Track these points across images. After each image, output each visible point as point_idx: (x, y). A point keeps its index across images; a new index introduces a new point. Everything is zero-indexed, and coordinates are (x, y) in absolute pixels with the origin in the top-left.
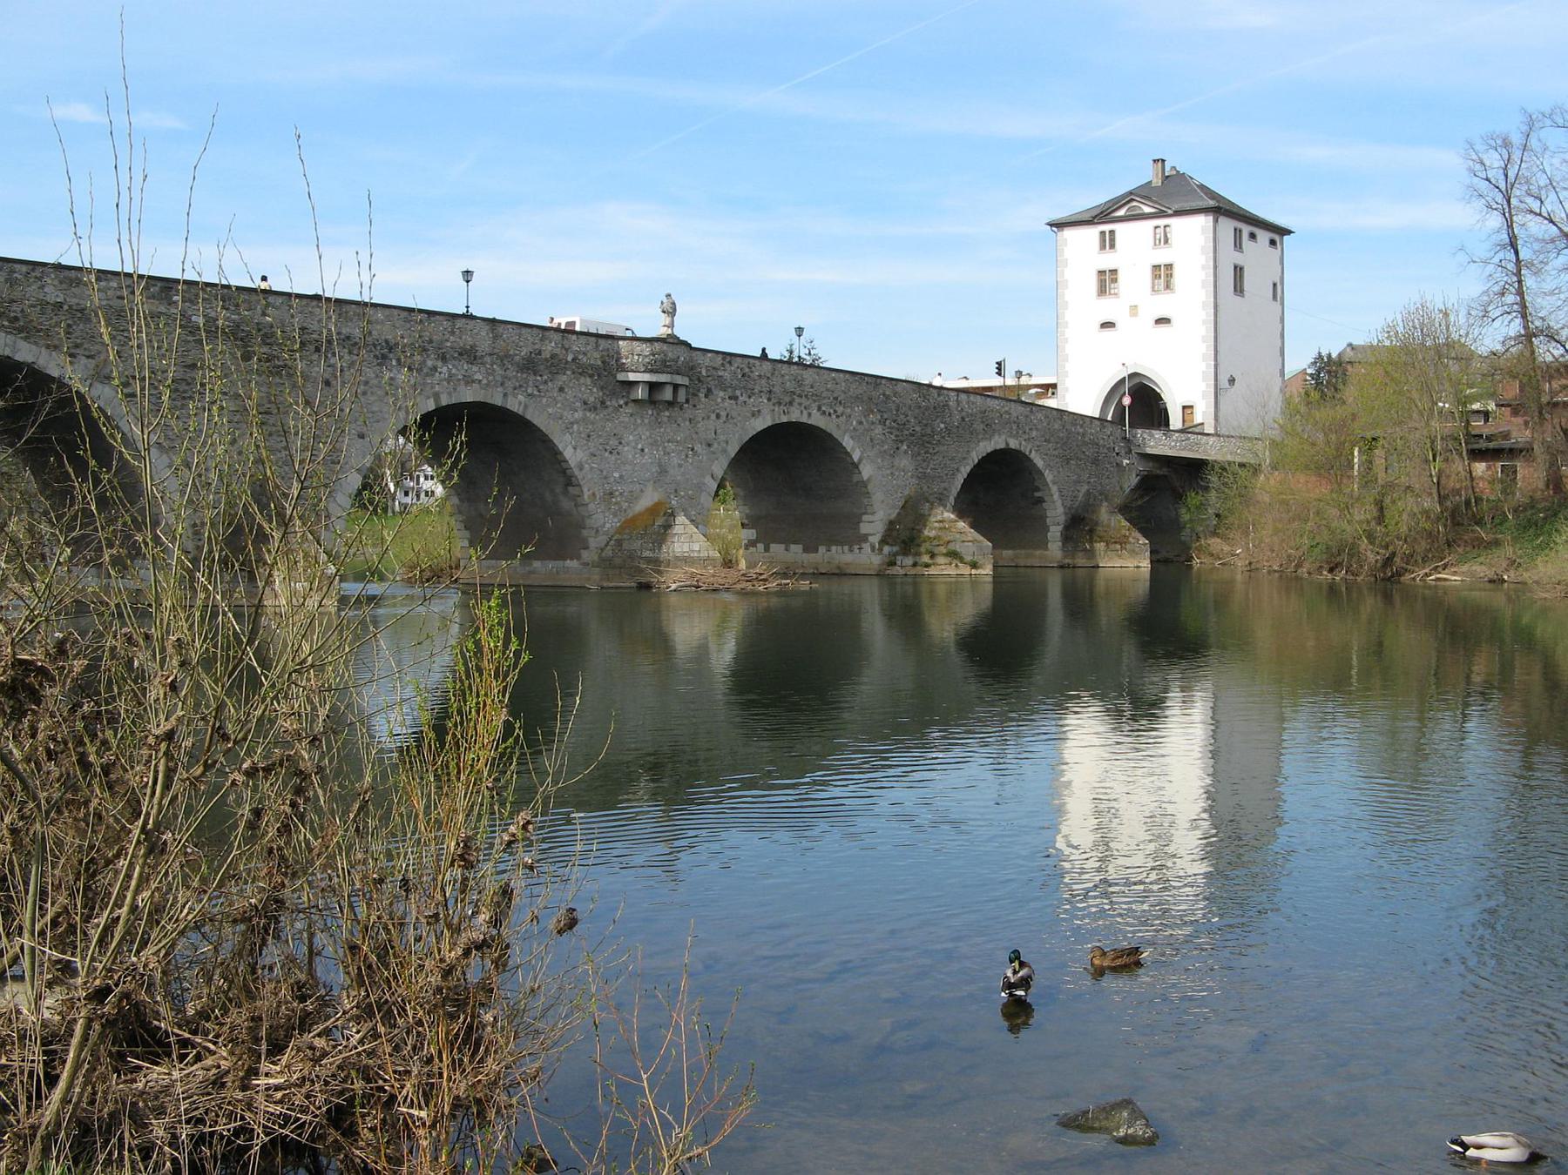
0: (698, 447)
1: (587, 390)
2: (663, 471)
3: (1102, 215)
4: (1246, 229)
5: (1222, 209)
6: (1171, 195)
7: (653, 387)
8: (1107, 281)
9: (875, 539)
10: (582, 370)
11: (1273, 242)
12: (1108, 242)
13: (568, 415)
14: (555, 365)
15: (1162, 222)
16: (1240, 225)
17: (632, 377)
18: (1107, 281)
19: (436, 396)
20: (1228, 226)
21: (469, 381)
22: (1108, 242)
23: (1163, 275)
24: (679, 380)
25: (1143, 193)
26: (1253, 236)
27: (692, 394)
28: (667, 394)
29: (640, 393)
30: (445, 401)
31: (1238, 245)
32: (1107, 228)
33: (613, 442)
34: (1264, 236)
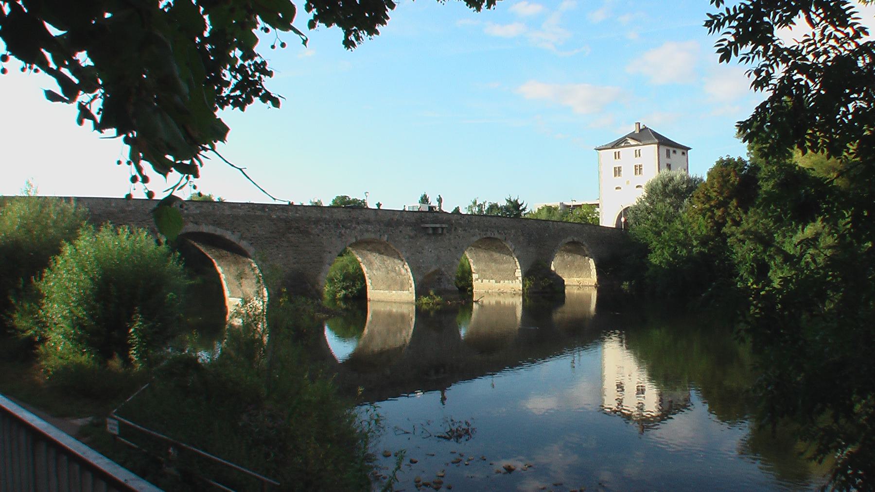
0: (452, 249)
1: (409, 231)
2: (439, 258)
3: (616, 145)
4: (671, 150)
5: (663, 142)
6: (643, 135)
7: (435, 229)
8: (618, 171)
9: (520, 278)
10: (408, 224)
11: (683, 153)
12: (617, 156)
13: (403, 241)
14: (398, 223)
15: (638, 148)
16: (669, 148)
17: (427, 226)
18: (618, 171)
19: (356, 237)
20: (664, 149)
21: (367, 231)
22: (617, 156)
23: (638, 169)
24: (444, 226)
25: (632, 136)
26: (674, 152)
27: (449, 231)
28: (440, 232)
29: (431, 232)
30: (359, 238)
31: (668, 156)
32: (617, 150)
33: (420, 249)
34: (679, 152)
